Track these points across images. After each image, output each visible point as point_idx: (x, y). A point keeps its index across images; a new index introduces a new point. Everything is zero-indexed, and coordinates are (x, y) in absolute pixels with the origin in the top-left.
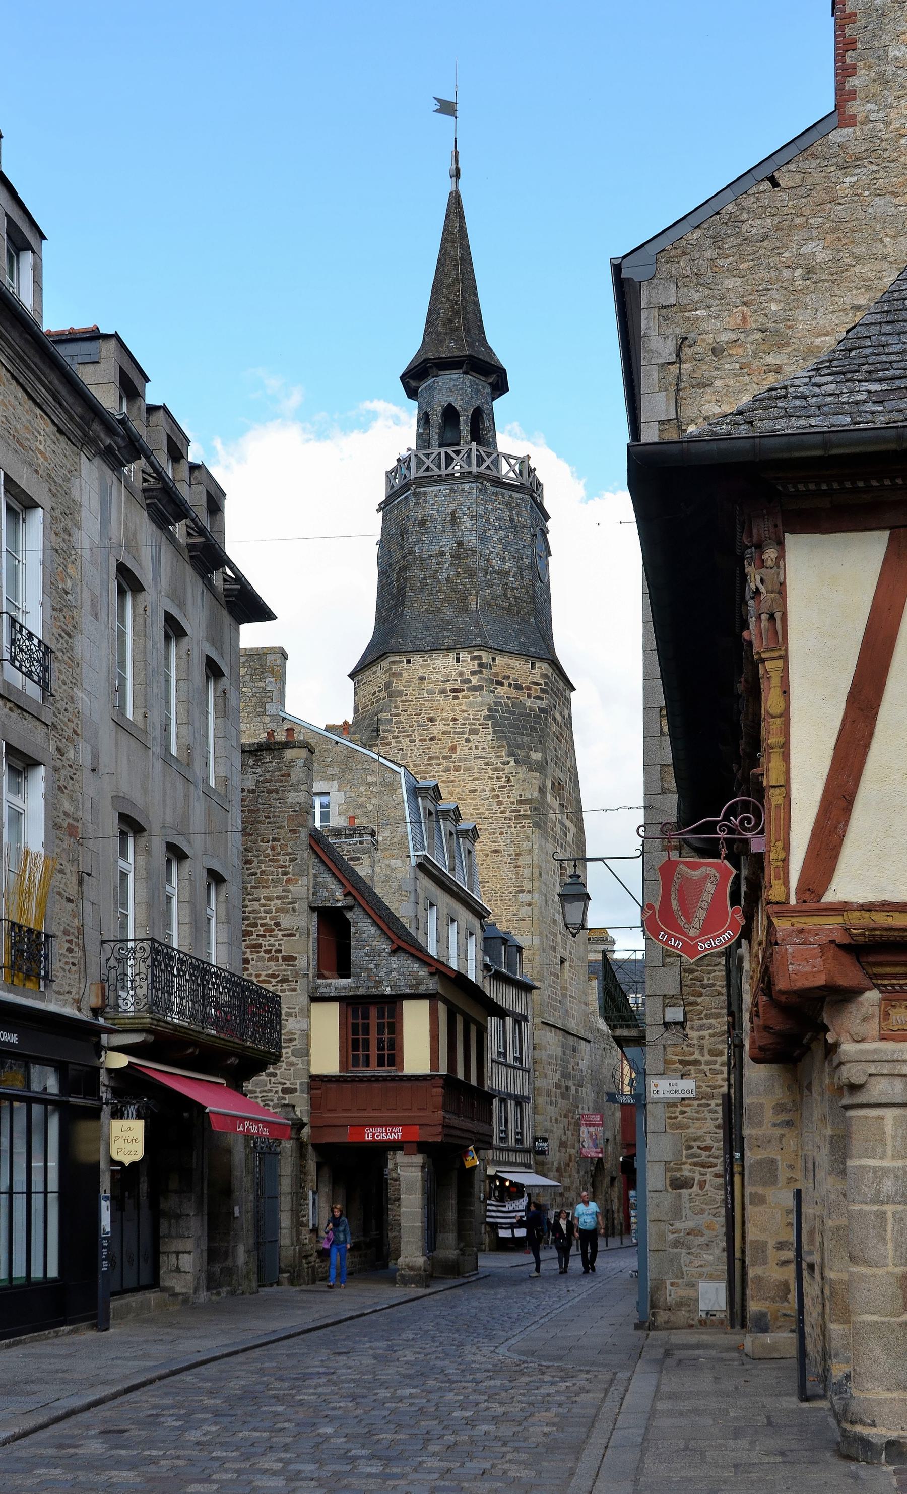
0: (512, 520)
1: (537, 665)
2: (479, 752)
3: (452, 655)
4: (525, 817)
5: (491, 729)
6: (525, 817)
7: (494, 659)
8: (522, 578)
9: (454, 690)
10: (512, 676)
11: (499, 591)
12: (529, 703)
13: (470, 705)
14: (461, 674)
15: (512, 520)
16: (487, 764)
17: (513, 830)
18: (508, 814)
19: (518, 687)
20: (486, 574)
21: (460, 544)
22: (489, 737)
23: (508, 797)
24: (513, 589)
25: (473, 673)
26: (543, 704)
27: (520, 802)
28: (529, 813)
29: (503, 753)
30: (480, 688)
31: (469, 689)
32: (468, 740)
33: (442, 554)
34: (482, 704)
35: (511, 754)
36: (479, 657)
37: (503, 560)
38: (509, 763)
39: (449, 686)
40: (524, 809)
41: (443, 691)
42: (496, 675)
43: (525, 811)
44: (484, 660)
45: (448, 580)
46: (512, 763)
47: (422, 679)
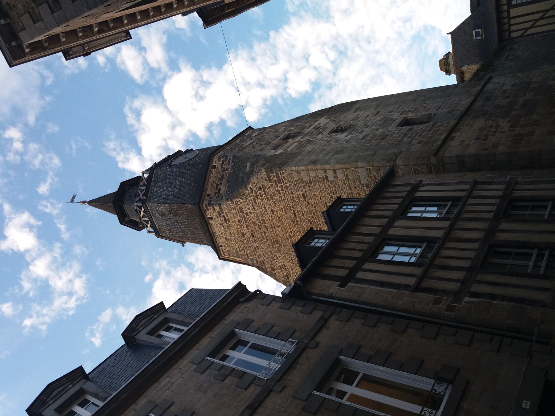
0: (161, 181)
1: (214, 164)
2: (251, 207)
3: (210, 221)
4: (278, 177)
5: (237, 200)
6: (278, 177)
7: (208, 195)
8: (183, 173)
10: (217, 182)
16: (256, 203)
17: (288, 185)
18: (279, 189)
19: (222, 178)
20: (179, 197)
22: (241, 201)
23: (270, 188)
24: (187, 179)
25: (214, 210)
28: (274, 174)
29: (247, 192)
31: (223, 213)
34: (226, 205)
36: (206, 205)
38: (251, 188)
39: (225, 224)
42: (215, 194)
43: (274, 177)
44: (207, 203)
46: (250, 186)
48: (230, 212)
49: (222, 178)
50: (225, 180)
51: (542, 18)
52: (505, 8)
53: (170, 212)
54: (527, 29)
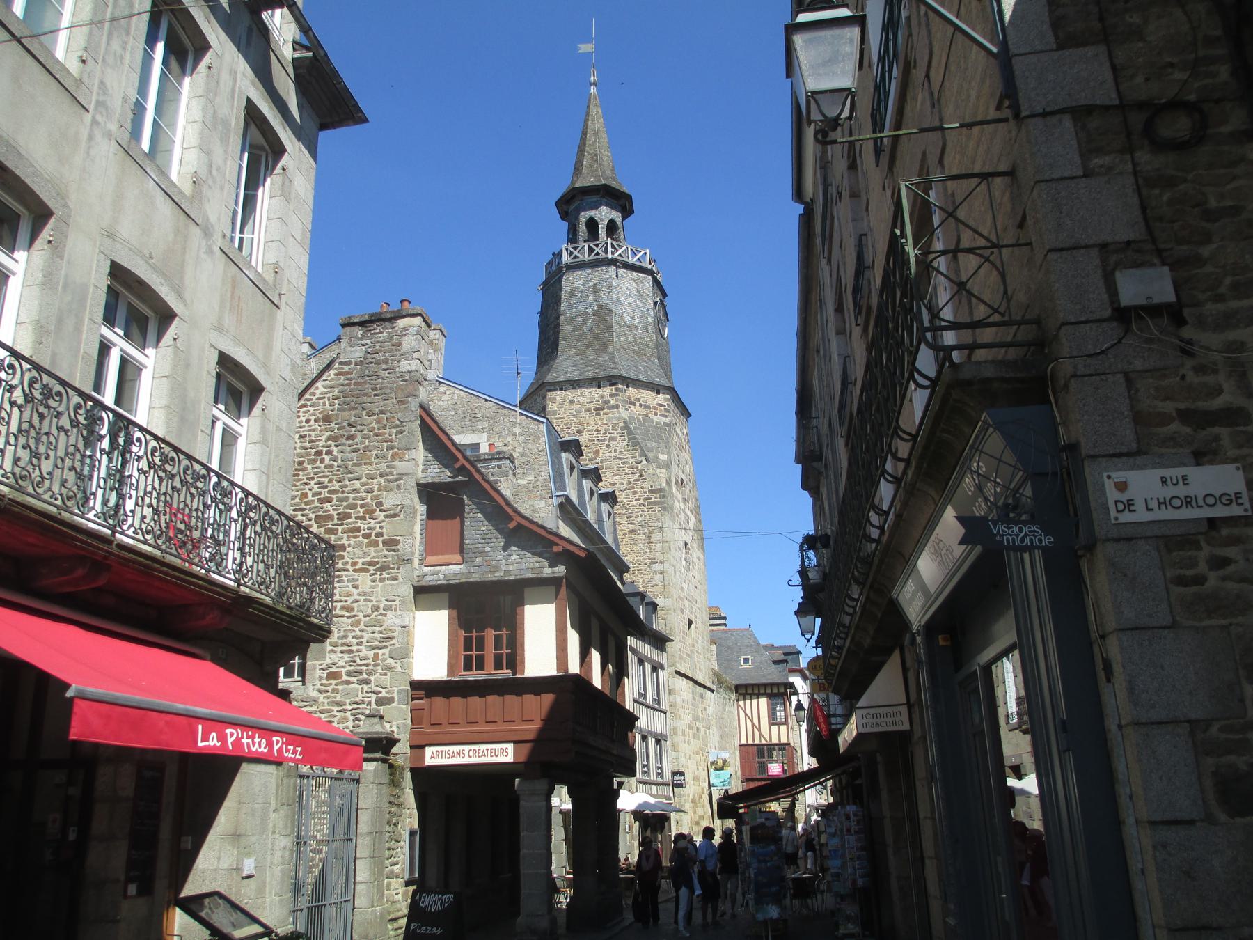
2: (617, 455)
4: (656, 503)
6: (656, 503)
9: (597, 409)
11: (630, 338)
12: (656, 418)
13: (609, 419)
14: (602, 397)
15: (639, 291)
19: (647, 407)
21: (600, 306)
25: (611, 396)
26: (667, 420)
27: (651, 491)
30: (617, 407)
32: (608, 446)
33: (587, 313)
34: (619, 418)
35: (643, 454)
37: (633, 317)
39: (592, 406)
40: (655, 497)
41: (588, 410)
45: (592, 332)
47: (571, 402)
48: (609, 419)
49: (647, 407)
50: (644, 412)
51: (753, 725)
52: (769, 691)
53: (600, 306)
54: (745, 711)
